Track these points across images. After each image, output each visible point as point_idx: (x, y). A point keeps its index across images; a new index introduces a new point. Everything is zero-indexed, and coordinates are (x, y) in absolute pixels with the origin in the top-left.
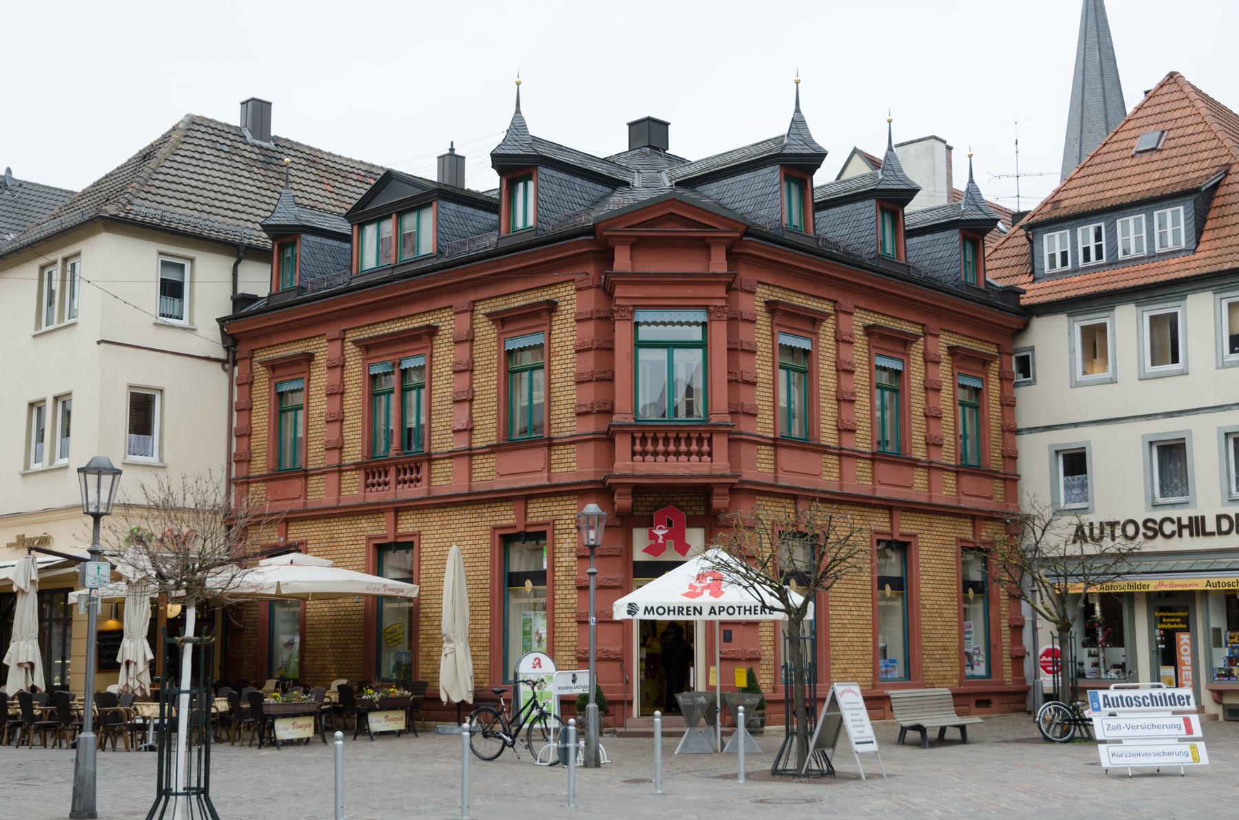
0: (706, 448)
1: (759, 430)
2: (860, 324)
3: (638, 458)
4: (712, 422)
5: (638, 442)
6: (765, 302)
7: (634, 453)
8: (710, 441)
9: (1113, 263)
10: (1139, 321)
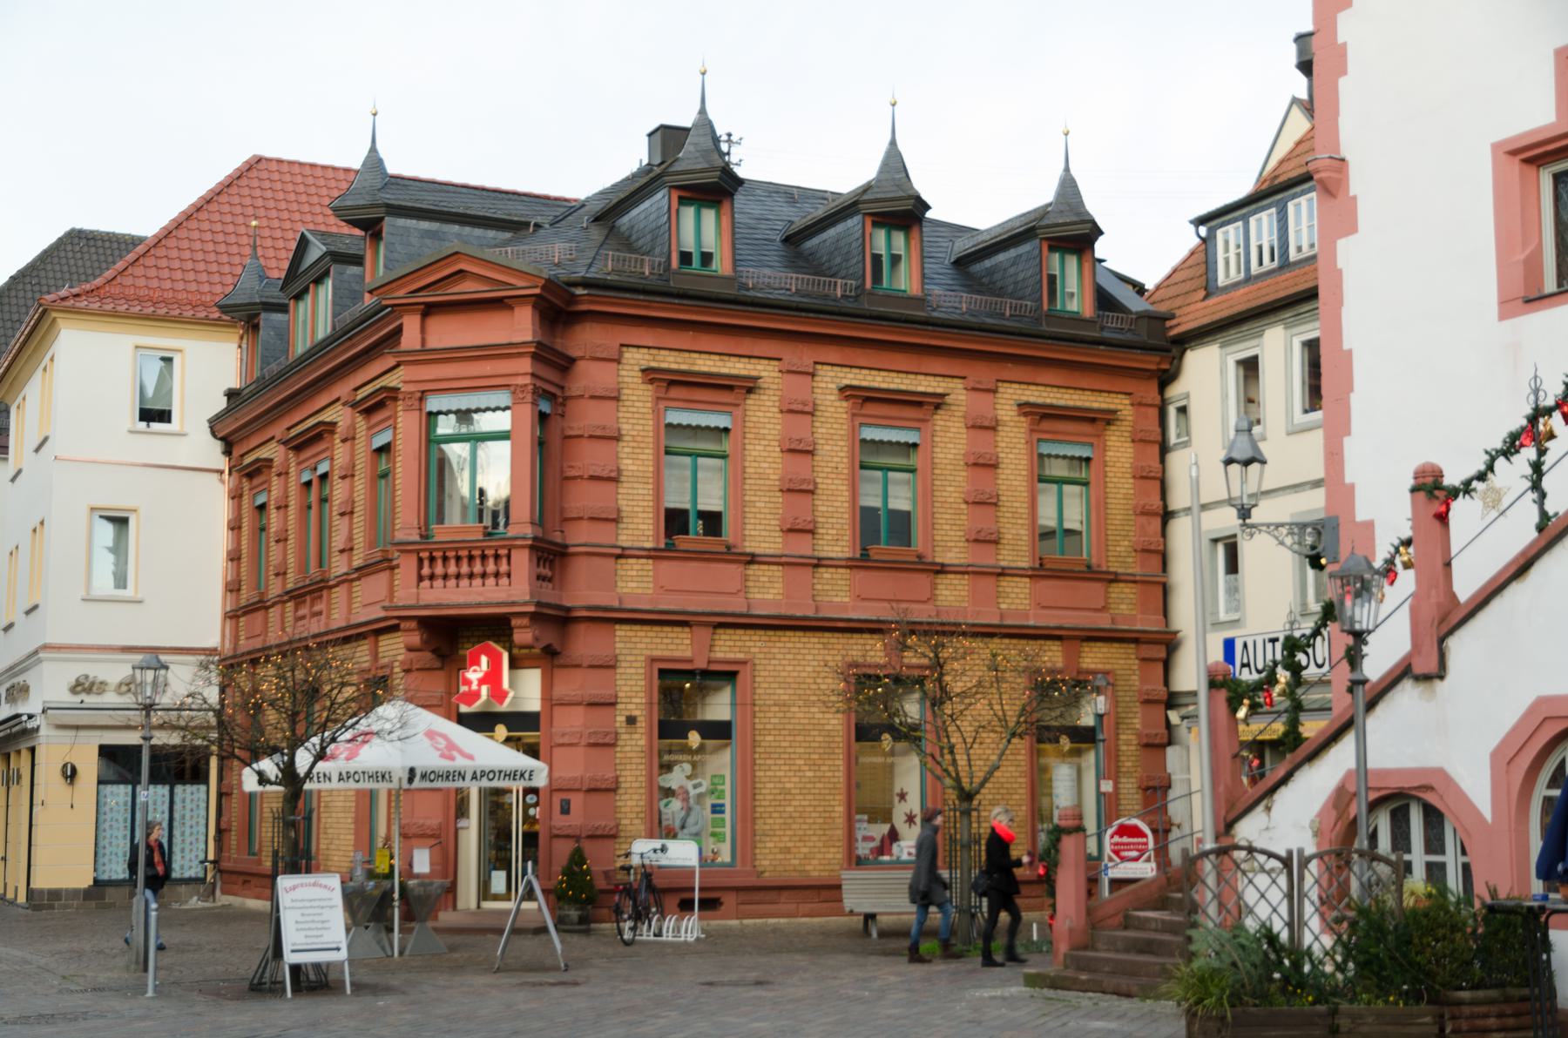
0: (504, 568)
1: (625, 540)
2: (834, 386)
3: (426, 583)
4: (509, 535)
5: (426, 563)
6: (643, 371)
7: (421, 578)
8: (509, 557)
9: (1285, 265)
10: (1289, 349)
